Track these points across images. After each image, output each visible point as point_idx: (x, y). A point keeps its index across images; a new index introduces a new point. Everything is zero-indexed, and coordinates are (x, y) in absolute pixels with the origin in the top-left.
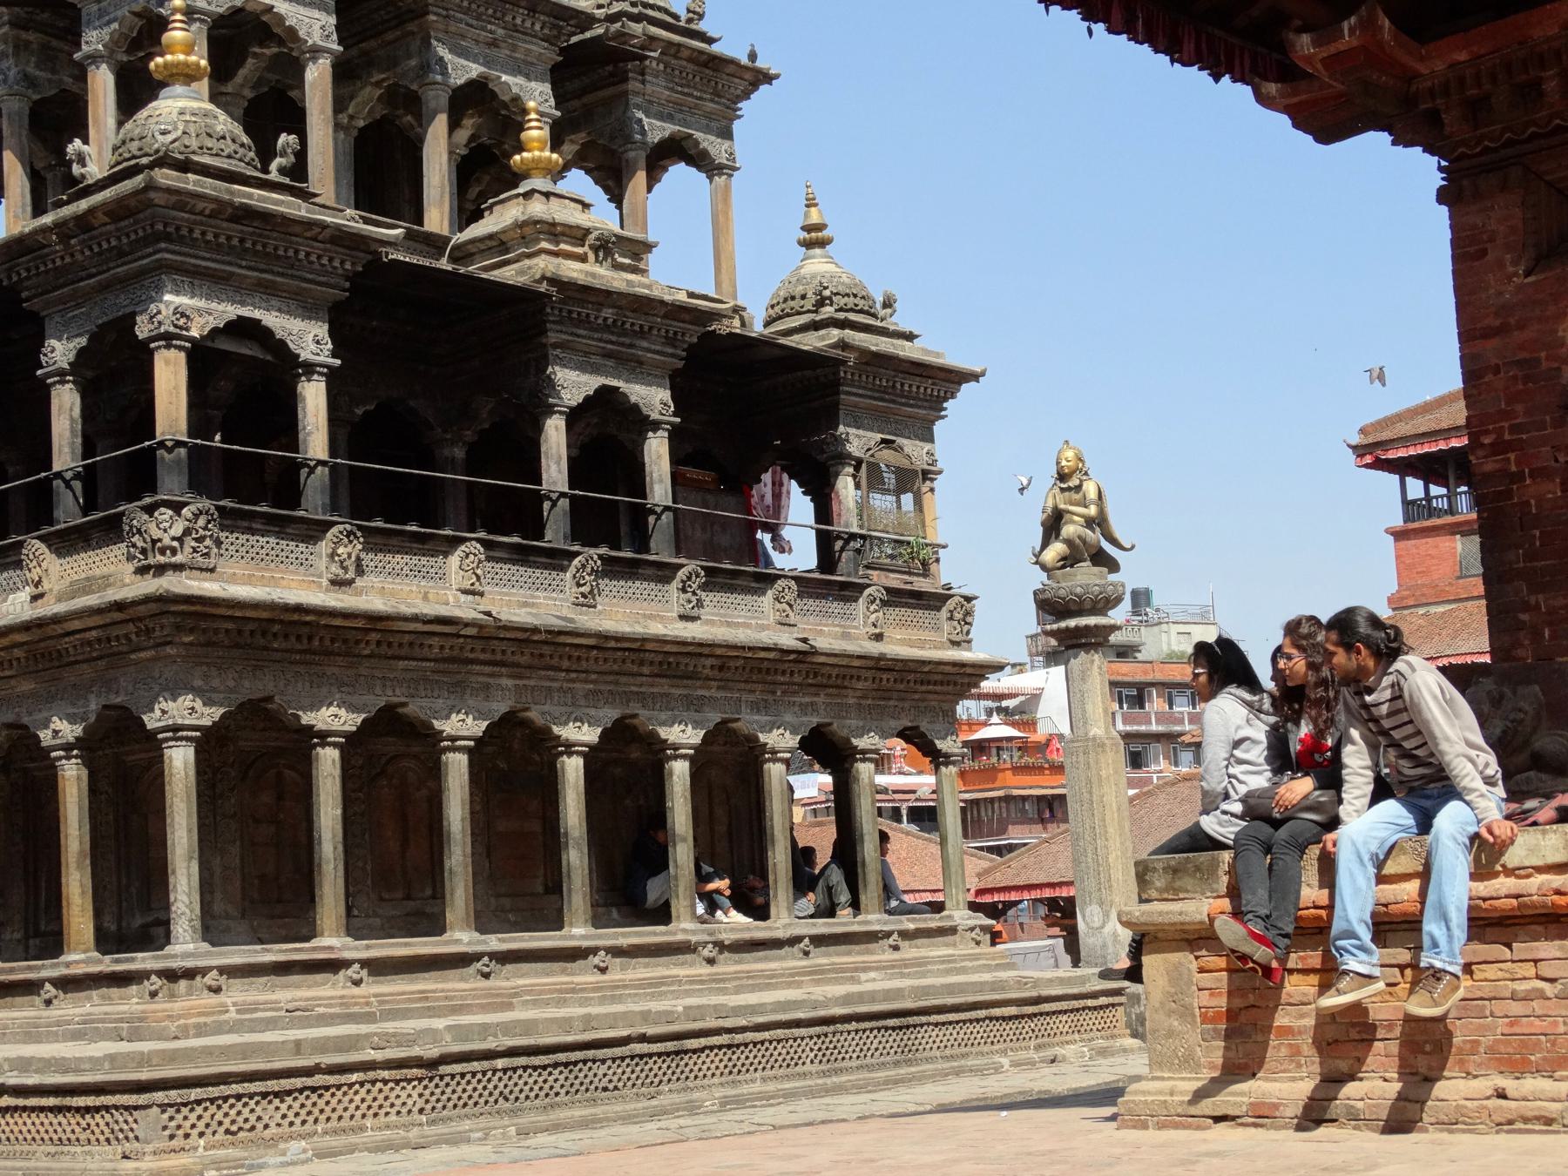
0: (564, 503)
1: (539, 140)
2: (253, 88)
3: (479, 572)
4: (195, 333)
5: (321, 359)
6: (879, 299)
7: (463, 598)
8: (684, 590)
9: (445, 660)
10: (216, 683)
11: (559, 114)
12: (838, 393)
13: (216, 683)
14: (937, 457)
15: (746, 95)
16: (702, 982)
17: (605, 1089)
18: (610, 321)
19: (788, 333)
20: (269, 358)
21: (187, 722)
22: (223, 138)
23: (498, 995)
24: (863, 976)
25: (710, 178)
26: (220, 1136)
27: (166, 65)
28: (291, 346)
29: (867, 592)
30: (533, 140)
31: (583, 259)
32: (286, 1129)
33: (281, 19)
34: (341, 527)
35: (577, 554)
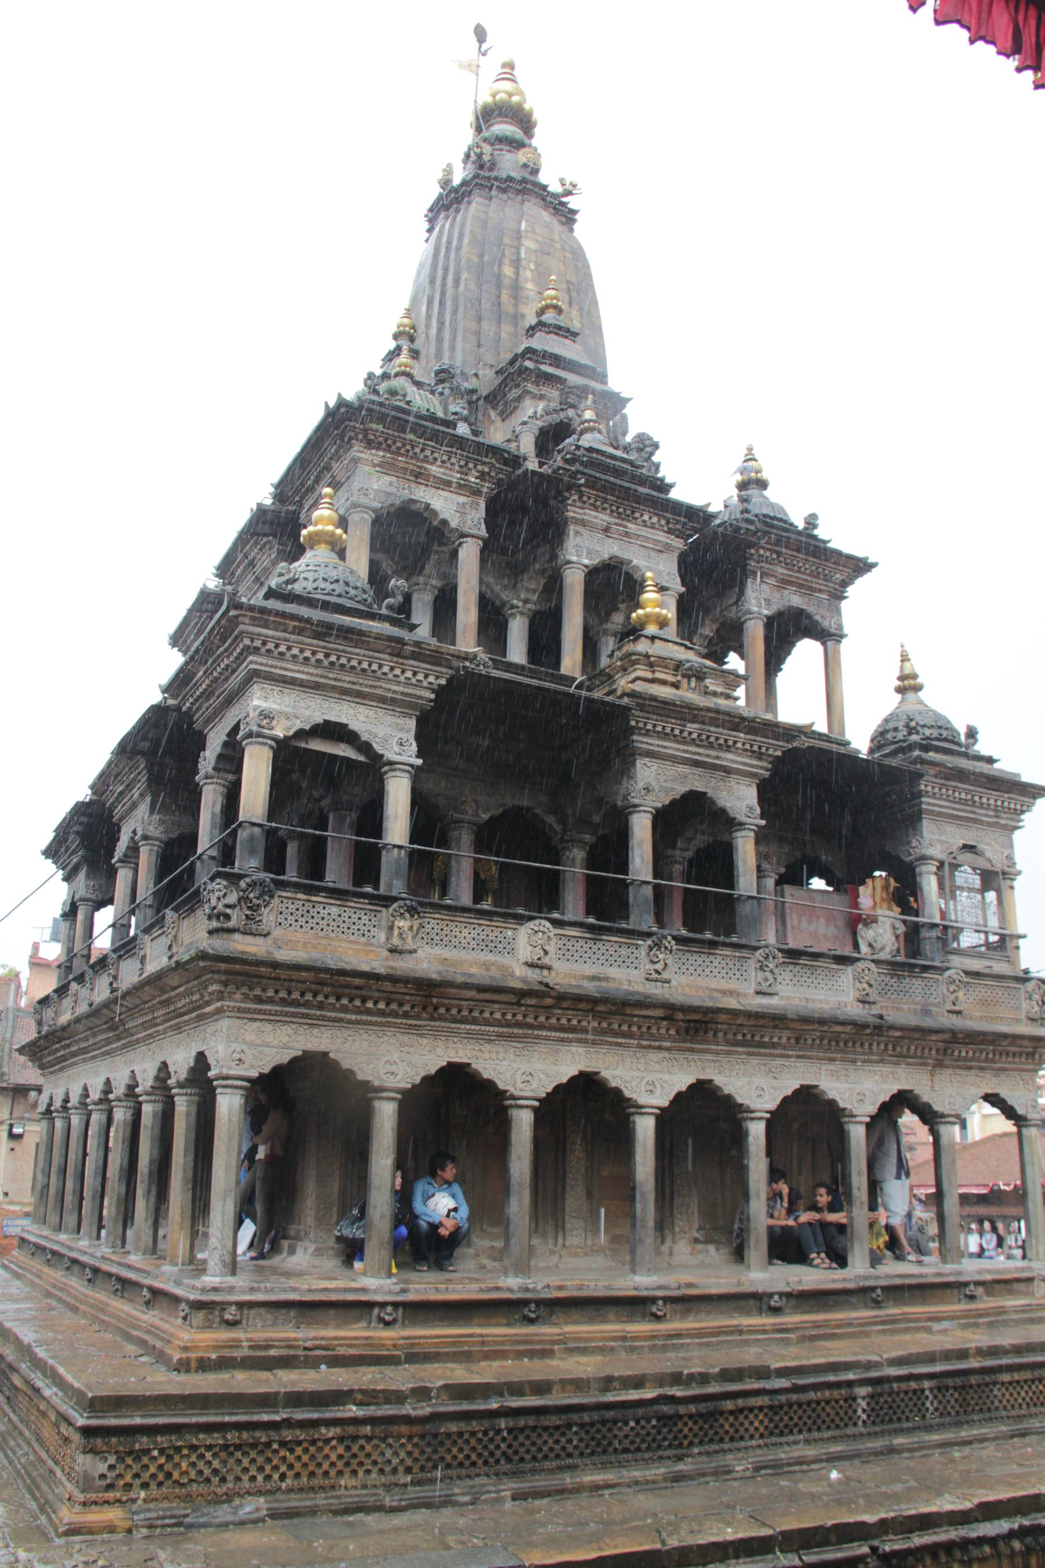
0: (649, 891)
1: (654, 601)
4: (280, 733)
6: (962, 731)
8: (761, 968)
9: (508, 1025)
10: (269, 1038)
12: (921, 803)
16: (765, 1332)
17: (626, 1450)
18: (694, 736)
19: (885, 756)
21: (232, 1072)
22: (337, 581)
23: (540, 1342)
24: (936, 1326)
25: (824, 644)
27: (310, 534)
28: (375, 746)
29: (948, 973)
30: (649, 600)
31: (676, 686)
32: (246, 1484)
33: (435, 513)
34: (401, 903)
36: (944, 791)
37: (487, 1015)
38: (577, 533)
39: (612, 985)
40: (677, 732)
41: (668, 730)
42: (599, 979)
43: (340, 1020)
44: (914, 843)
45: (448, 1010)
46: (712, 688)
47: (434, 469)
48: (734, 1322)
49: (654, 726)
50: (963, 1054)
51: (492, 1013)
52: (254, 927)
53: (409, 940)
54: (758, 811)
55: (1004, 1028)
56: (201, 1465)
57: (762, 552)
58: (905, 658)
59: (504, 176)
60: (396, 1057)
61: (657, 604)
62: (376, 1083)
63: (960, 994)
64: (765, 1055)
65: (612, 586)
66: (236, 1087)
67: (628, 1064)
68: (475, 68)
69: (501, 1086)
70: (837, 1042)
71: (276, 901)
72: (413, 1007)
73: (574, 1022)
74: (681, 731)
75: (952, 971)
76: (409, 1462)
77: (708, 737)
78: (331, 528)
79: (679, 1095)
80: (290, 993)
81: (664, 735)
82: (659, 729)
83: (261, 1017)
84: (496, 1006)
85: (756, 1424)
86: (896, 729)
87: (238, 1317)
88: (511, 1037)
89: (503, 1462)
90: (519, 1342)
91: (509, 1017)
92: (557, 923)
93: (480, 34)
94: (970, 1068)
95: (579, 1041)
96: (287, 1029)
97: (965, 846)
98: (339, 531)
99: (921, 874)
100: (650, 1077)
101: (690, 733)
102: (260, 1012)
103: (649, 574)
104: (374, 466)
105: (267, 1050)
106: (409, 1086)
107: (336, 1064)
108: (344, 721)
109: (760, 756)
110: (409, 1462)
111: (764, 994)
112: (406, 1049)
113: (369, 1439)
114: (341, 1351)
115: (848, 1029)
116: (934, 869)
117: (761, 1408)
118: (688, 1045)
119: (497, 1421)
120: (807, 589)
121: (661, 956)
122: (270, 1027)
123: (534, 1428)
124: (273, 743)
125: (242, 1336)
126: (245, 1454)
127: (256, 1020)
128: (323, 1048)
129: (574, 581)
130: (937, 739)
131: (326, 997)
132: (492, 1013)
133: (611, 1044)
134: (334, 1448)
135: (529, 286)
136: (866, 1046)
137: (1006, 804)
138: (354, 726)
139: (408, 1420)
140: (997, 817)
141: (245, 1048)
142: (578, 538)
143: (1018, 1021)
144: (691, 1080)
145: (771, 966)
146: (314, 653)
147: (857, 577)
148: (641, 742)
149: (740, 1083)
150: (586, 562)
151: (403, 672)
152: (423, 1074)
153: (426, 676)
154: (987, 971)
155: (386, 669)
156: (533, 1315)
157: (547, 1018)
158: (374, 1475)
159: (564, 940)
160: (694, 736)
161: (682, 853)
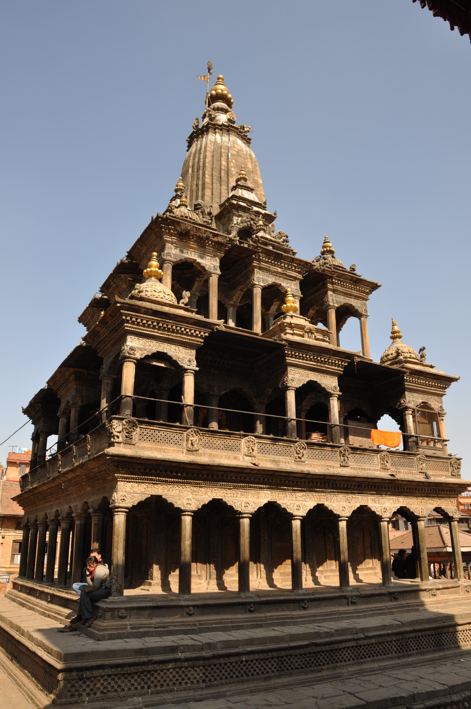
0: (294, 423)
2: (199, 292)
3: (254, 448)
7: (247, 458)
10: (136, 490)
11: (302, 296)
14: (444, 408)
15: (371, 292)
16: (350, 613)
20: (173, 368)
21: (120, 505)
25: (360, 319)
26: (99, 695)
30: (289, 300)
31: (302, 336)
35: (296, 442)
36: (414, 379)
37: (229, 478)
44: (402, 402)
45: (213, 476)
46: (318, 337)
48: (337, 609)
51: (231, 477)
52: (130, 440)
53: (196, 446)
54: (338, 389)
56: (112, 683)
57: (334, 280)
59: (221, 123)
60: (190, 496)
61: (293, 303)
62: (183, 508)
63: (424, 465)
65: (274, 294)
66: (123, 512)
67: (288, 498)
69: (236, 508)
70: (375, 487)
71: (138, 429)
73: (266, 480)
76: (204, 677)
78: (157, 269)
79: (310, 510)
80: (145, 470)
84: (233, 474)
85: (347, 655)
86: (392, 354)
87: (125, 615)
89: (244, 675)
90: (247, 622)
96: (144, 486)
98: (160, 271)
99: (405, 415)
100: (298, 503)
102: (132, 478)
103: (289, 289)
105: (135, 495)
106: (197, 509)
107: (165, 500)
108: (165, 351)
110: (204, 677)
112: (195, 493)
113: (186, 668)
114: (172, 628)
116: (411, 412)
117: (352, 647)
119: (241, 657)
122: (137, 485)
123: (257, 660)
124: (135, 361)
125: (128, 623)
126: (133, 677)
128: (159, 494)
129: (258, 292)
130: (410, 358)
131: (161, 471)
132: (231, 477)
134: (171, 673)
135: (233, 169)
138: (170, 353)
139: (203, 658)
141: (126, 494)
144: (315, 504)
145: (346, 454)
147: (373, 291)
148: (289, 360)
150: (262, 284)
152: (202, 504)
154: (435, 455)
155: (183, 329)
156: (252, 609)
158: (189, 685)
159: (261, 445)
161: (306, 406)
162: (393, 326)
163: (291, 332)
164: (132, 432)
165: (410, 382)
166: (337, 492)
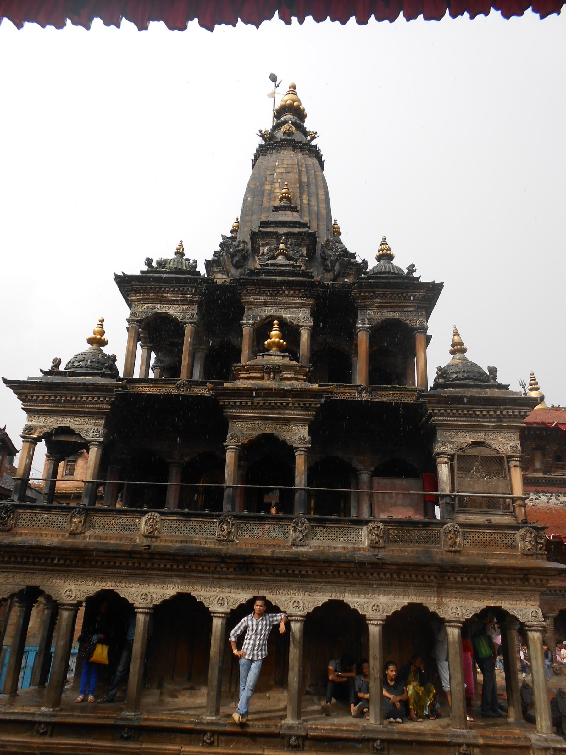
1: (275, 335)
5: (94, 439)
13: (11, 580)
28: (82, 435)
31: (262, 378)
33: (171, 316)
38: (249, 309)
39: (194, 545)
40: (249, 404)
41: (244, 404)
42: (187, 542)
43: (45, 570)
46: (286, 376)
47: (169, 296)
49: (235, 403)
50: (459, 579)
55: (492, 562)
57: (362, 294)
58: (456, 333)
60: (73, 587)
63: (458, 540)
64: (301, 581)
68: (273, 95)
72: (78, 561)
74: (252, 403)
75: (449, 525)
77: (270, 403)
80: (16, 558)
81: (241, 407)
82: (238, 404)
83: (6, 570)
88: (136, 575)
91: (130, 564)
92: (162, 514)
93: (273, 78)
94: (472, 589)
95: (177, 576)
97: (473, 443)
100: (221, 595)
101: (258, 403)
104: (140, 301)
108: (68, 425)
109: (307, 409)
111: (298, 546)
115: (353, 565)
118: (246, 577)
120: (393, 308)
121: (226, 527)
127: (5, 572)
128: (37, 584)
132: (121, 563)
133: (197, 577)
136: (375, 575)
137: (505, 413)
138: (73, 427)
140: (501, 422)
142: (250, 312)
143: (514, 557)
146: (50, 397)
149: (284, 599)
151: (93, 398)
152: (86, 596)
153: (99, 398)
156: (125, 735)
157: (153, 564)
160: (261, 404)
162: (454, 336)
163: (246, 376)
164: (5, 517)
165: (442, 415)
166: (288, 581)
